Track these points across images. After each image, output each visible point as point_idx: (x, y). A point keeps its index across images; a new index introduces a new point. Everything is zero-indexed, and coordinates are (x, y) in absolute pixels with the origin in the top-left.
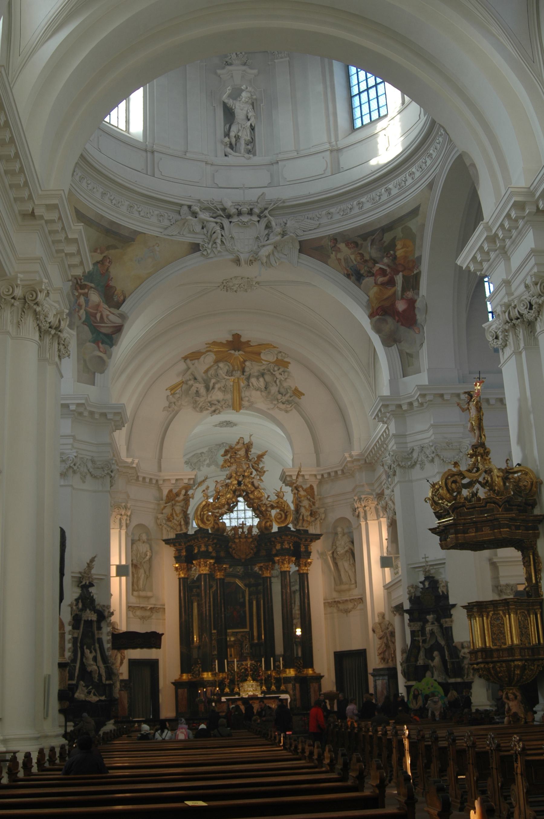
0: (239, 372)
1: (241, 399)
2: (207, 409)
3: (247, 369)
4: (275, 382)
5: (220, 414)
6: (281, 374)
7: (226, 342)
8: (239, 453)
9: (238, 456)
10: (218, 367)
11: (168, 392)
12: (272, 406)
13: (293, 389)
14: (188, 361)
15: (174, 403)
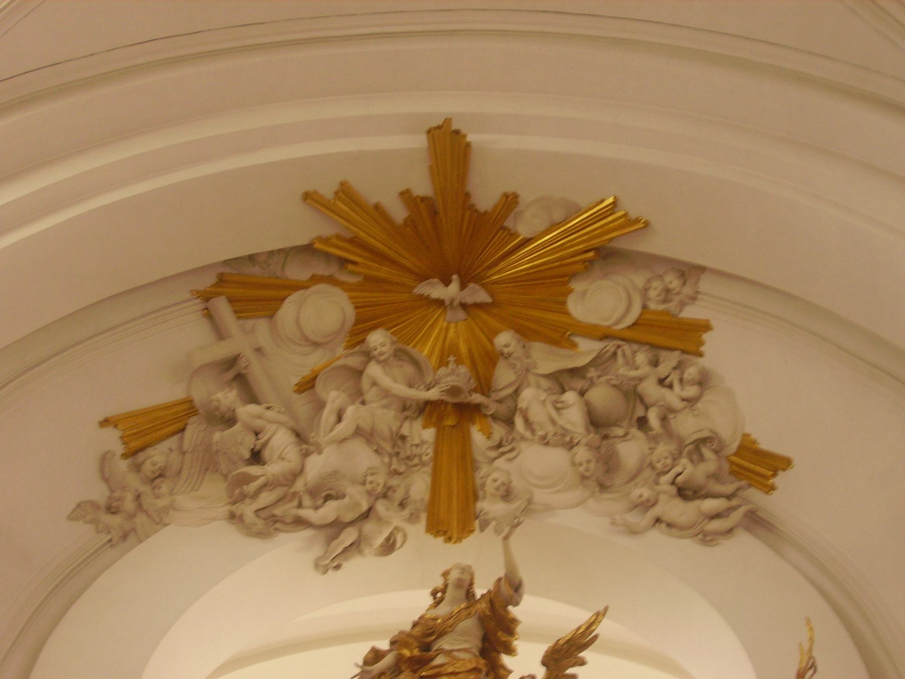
0: (463, 369)
1: (472, 495)
2: (300, 523)
3: (504, 376)
4: (642, 423)
5: (360, 552)
6: (671, 386)
7: (399, 213)
8: (445, 644)
9: (438, 661)
10: (368, 356)
11: (112, 440)
12: (633, 518)
13: (734, 446)
14: (222, 307)
15: (138, 497)
